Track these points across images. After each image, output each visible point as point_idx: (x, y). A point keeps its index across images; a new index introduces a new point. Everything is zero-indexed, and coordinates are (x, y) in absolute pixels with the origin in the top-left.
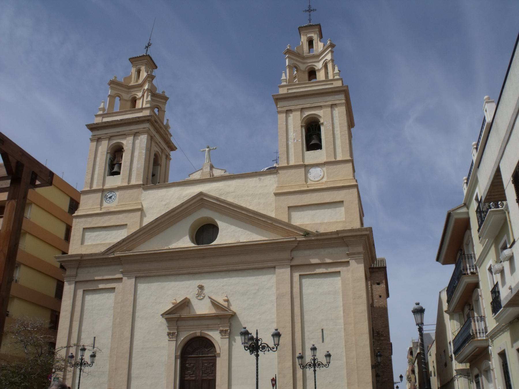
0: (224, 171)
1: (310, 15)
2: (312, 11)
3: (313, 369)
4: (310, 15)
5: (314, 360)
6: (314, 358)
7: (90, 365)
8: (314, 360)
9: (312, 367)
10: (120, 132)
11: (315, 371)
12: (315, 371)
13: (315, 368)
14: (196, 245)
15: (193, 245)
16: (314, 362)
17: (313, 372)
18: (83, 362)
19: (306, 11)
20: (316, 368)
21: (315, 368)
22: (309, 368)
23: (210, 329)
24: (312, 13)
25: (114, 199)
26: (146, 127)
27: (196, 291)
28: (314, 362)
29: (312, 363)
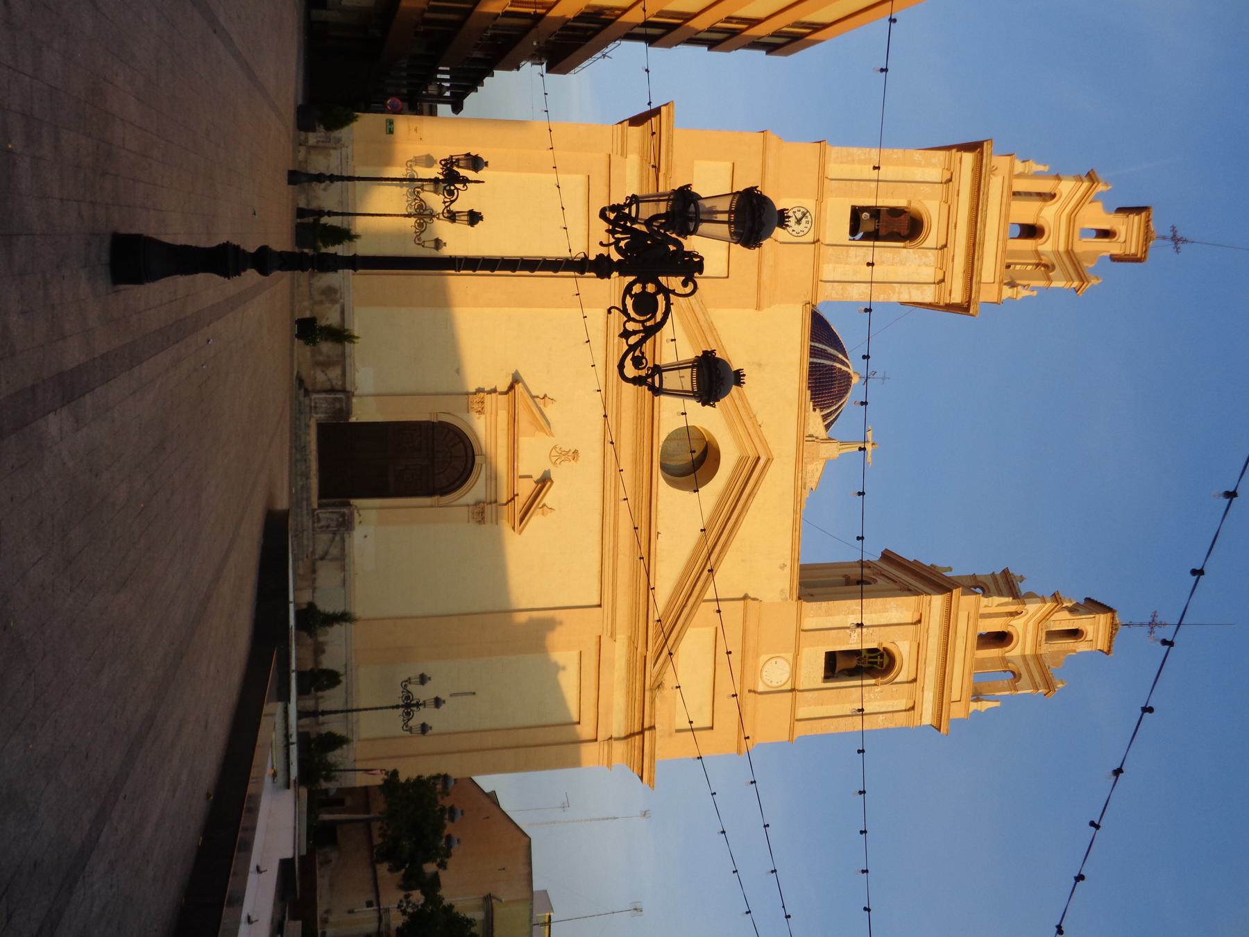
0: (814, 489)
1: (1141, 625)
2: (1149, 630)
3: (401, 703)
4: (1141, 625)
5: (418, 705)
6: (421, 705)
7: (419, 240)
8: (418, 705)
9: (404, 702)
10: (954, 230)
11: (397, 707)
12: (397, 707)
13: (402, 706)
14: (661, 444)
15: (663, 437)
16: (414, 705)
17: (395, 705)
18: (426, 220)
19: (1154, 616)
20: (401, 710)
21: (402, 706)
22: (402, 697)
23: (489, 482)
24: (1147, 629)
25: (793, 231)
26: (953, 295)
27: (569, 446)
28: (414, 705)
29: (411, 701)
